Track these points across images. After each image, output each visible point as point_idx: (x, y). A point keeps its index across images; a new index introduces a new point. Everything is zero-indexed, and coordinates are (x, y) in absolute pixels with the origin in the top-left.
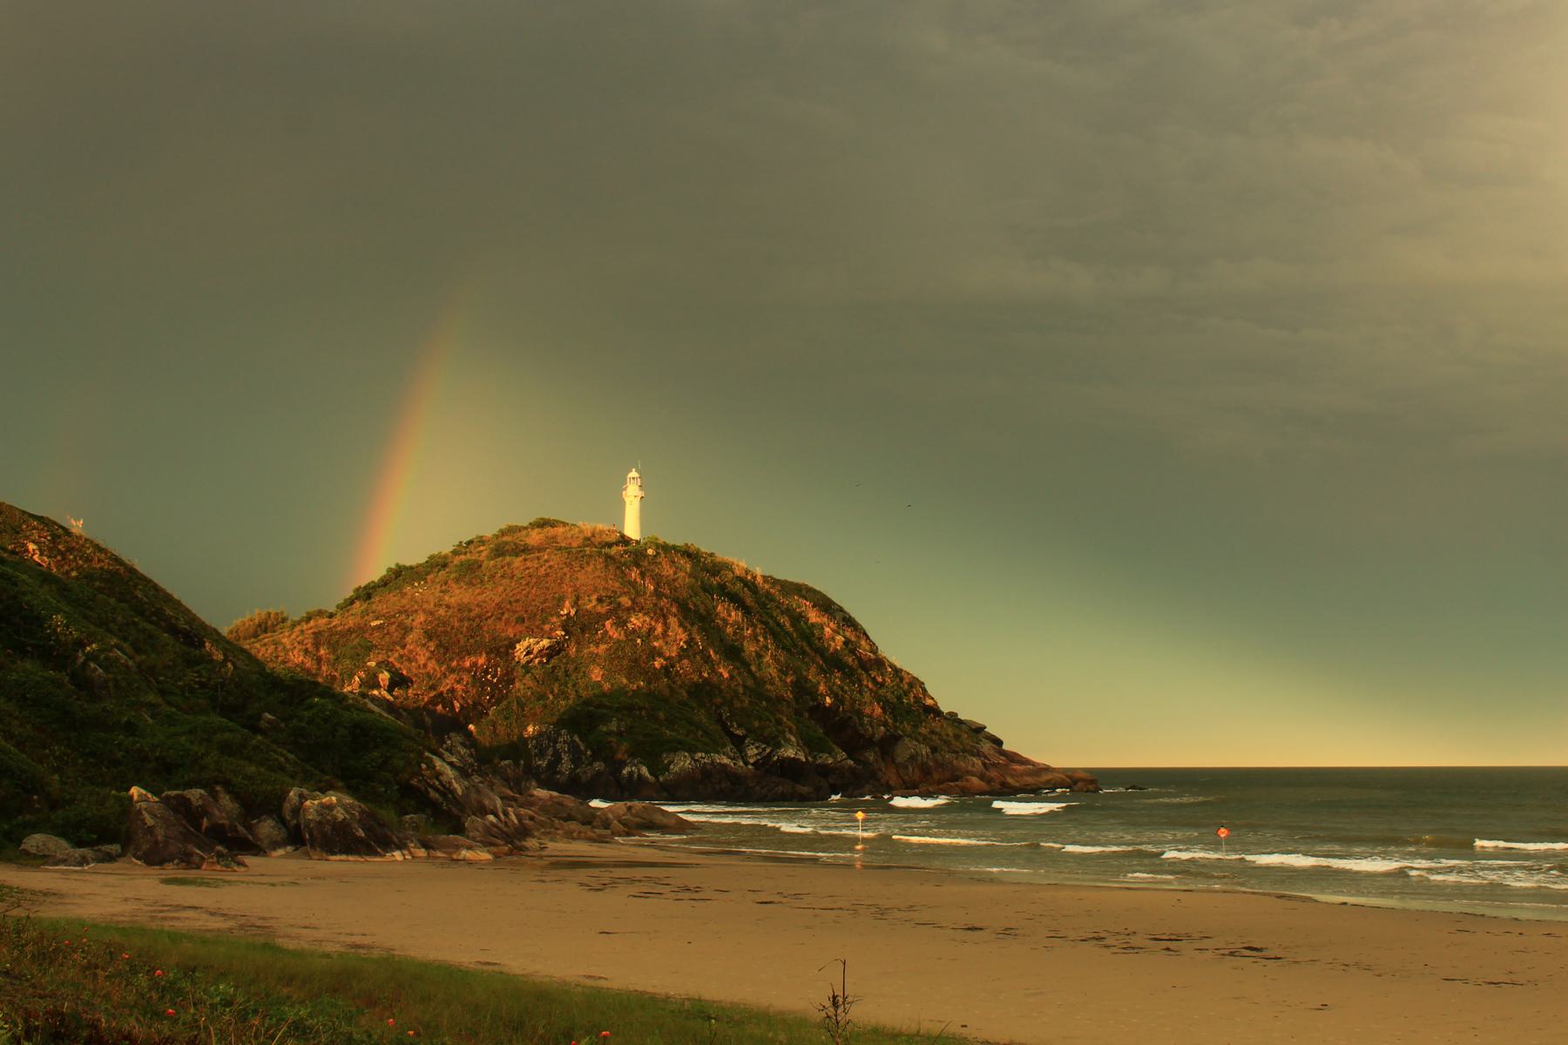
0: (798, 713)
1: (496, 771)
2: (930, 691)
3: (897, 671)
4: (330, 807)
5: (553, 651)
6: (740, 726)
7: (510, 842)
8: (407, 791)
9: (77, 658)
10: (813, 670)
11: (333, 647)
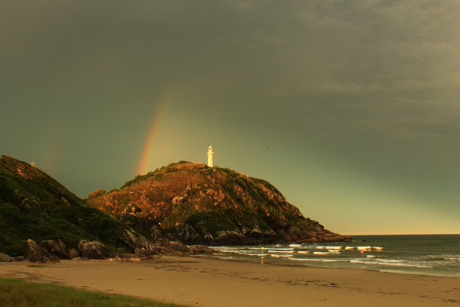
0: (259, 218)
1: (167, 237)
2: (301, 212)
3: (290, 206)
4: (91, 245)
5: (184, 201)
6: (240, 222)
7: (148, 256)
8: (119, 241)
9: (22, 202)
10: (264, 205)
11: (119, 200)
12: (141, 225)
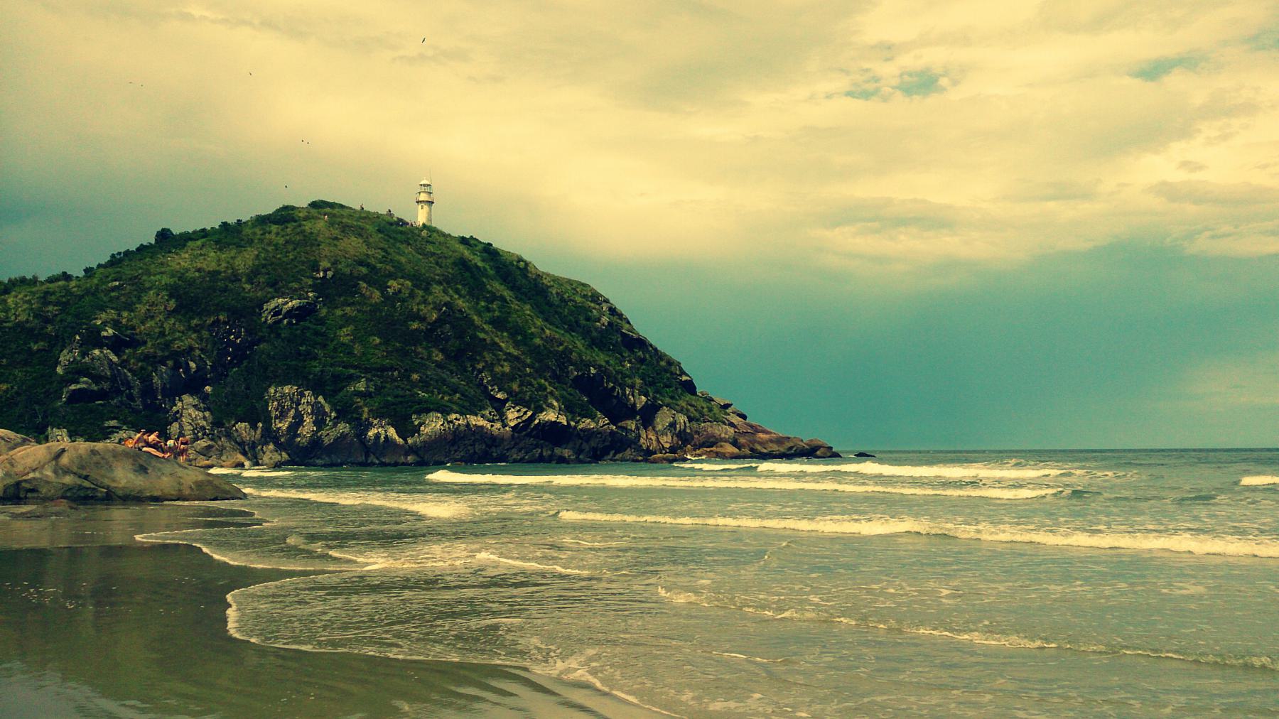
1: (229, 436)
12: (135, 392)
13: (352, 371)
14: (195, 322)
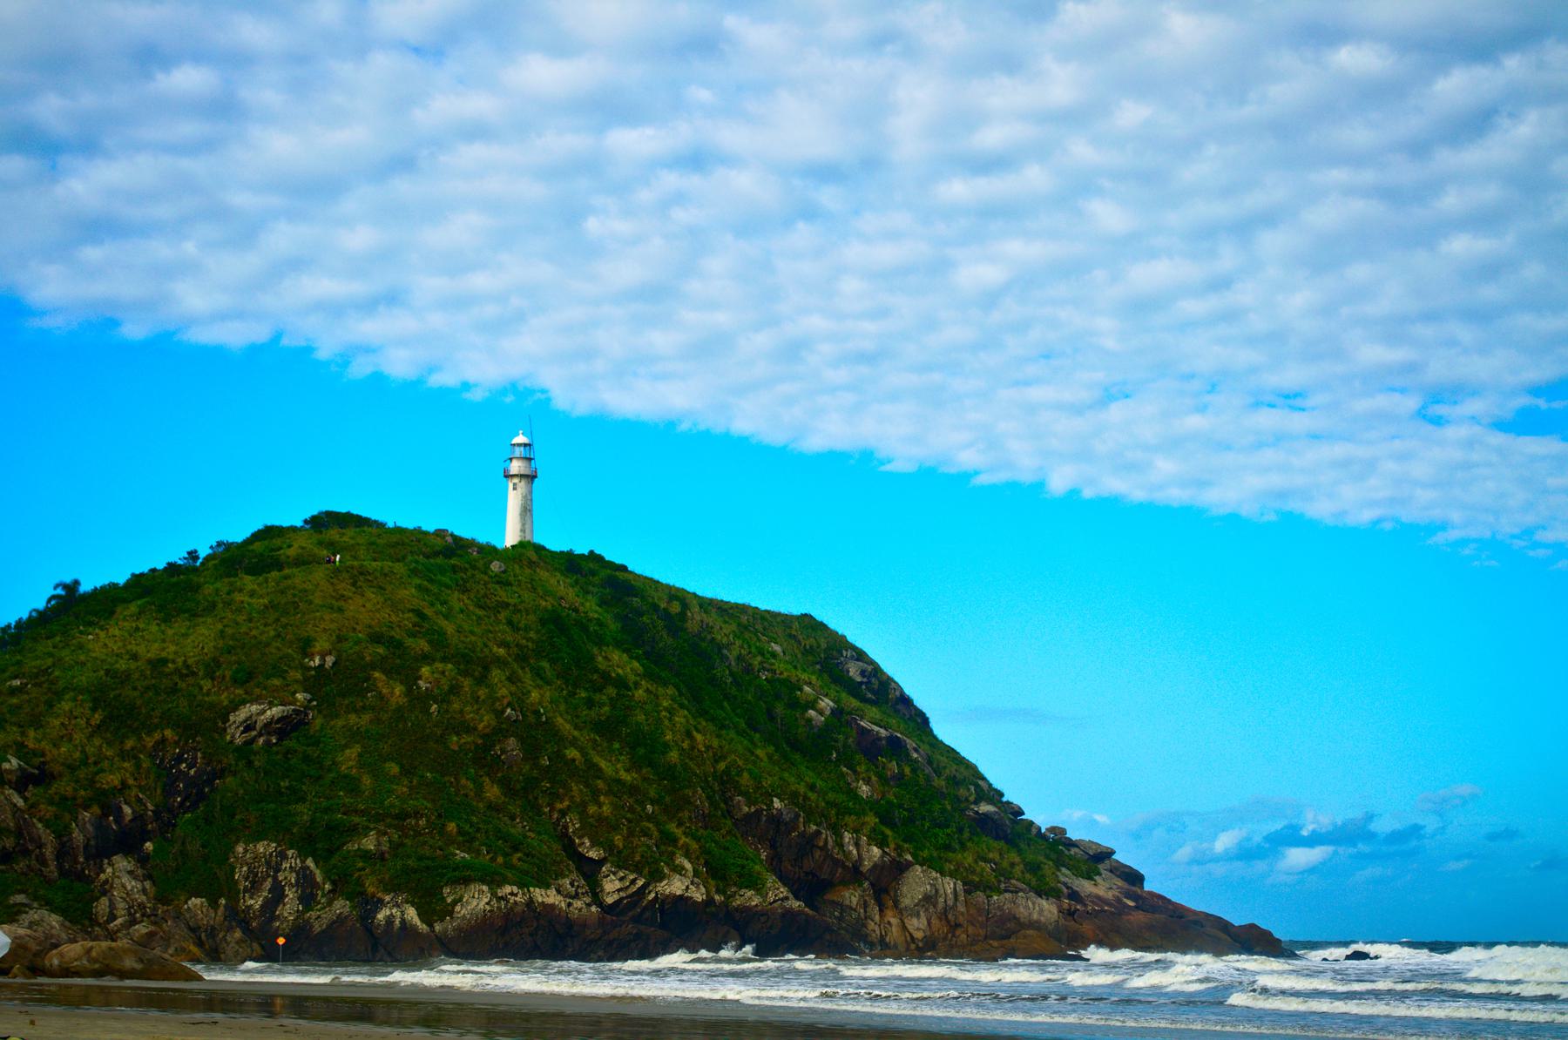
5: (286, 727)
13: (356, 819)
14: (129, 744)
